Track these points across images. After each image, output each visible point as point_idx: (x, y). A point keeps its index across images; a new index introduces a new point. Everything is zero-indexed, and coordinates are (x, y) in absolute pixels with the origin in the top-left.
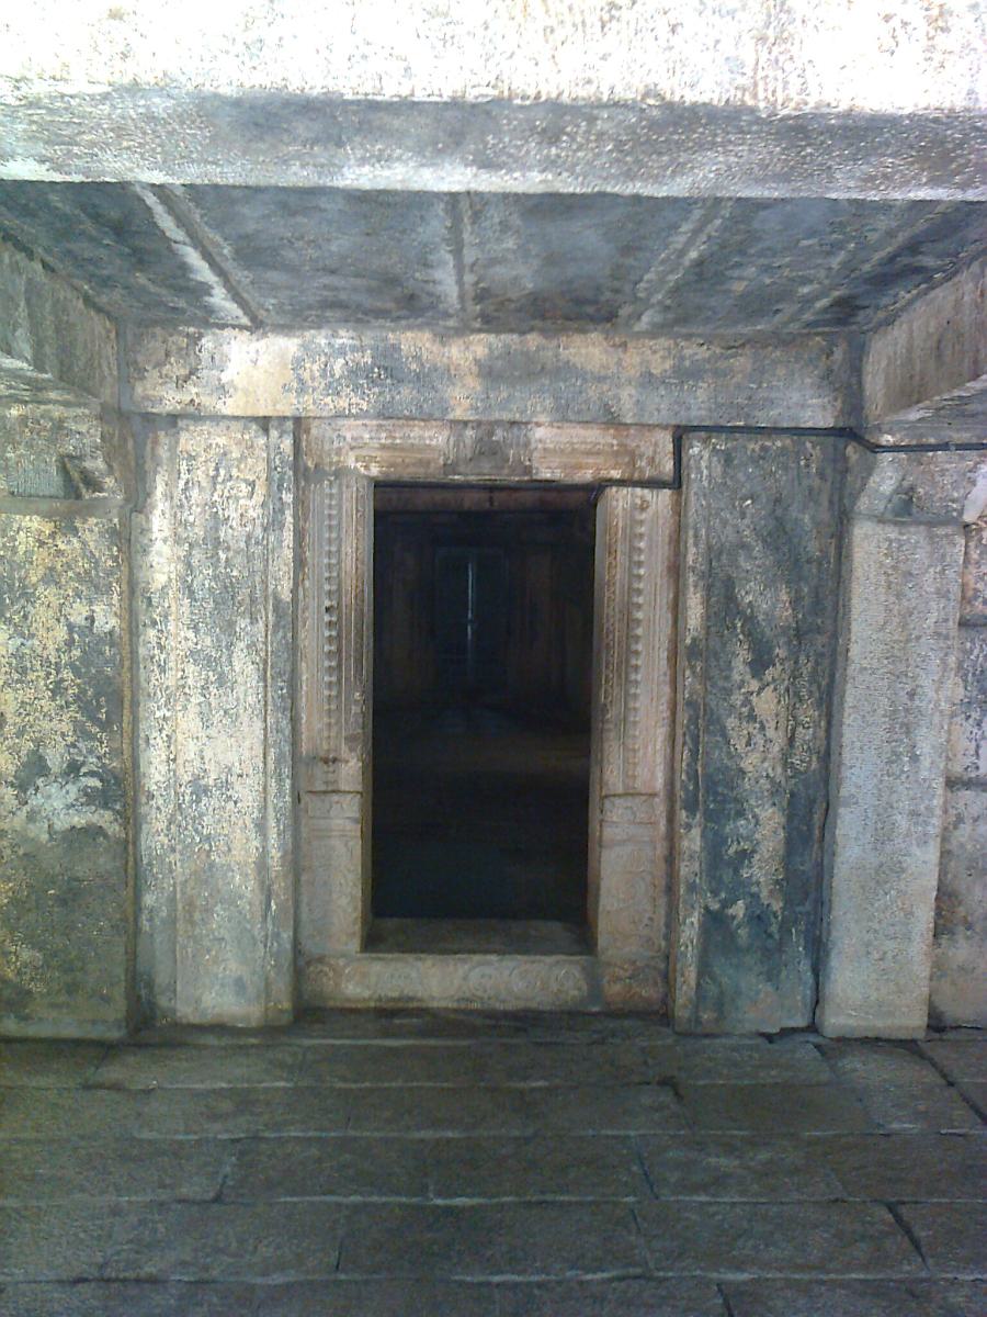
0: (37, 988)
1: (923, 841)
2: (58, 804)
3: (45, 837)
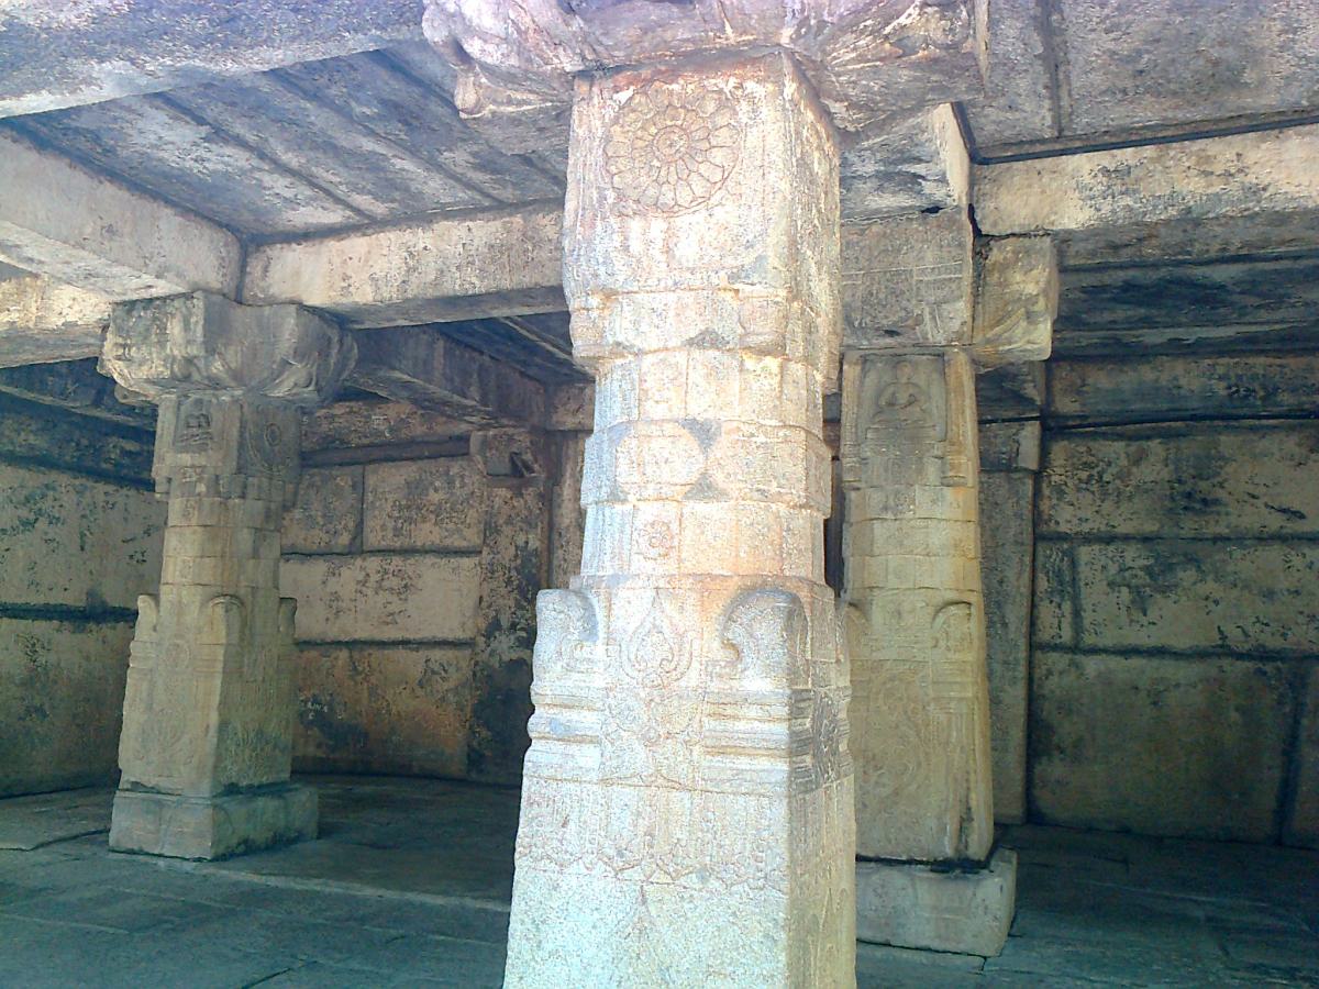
0: (488, 753)
1: (1014, 681)
2: (505, 647)
3: (497, 665)
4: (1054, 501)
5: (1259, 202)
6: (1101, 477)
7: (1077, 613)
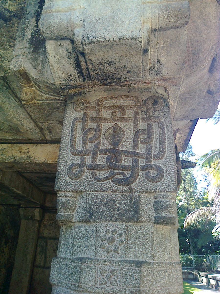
4: (44, 228)
5: (30, 160)
6: (55, 223)
7: (45, 258)
